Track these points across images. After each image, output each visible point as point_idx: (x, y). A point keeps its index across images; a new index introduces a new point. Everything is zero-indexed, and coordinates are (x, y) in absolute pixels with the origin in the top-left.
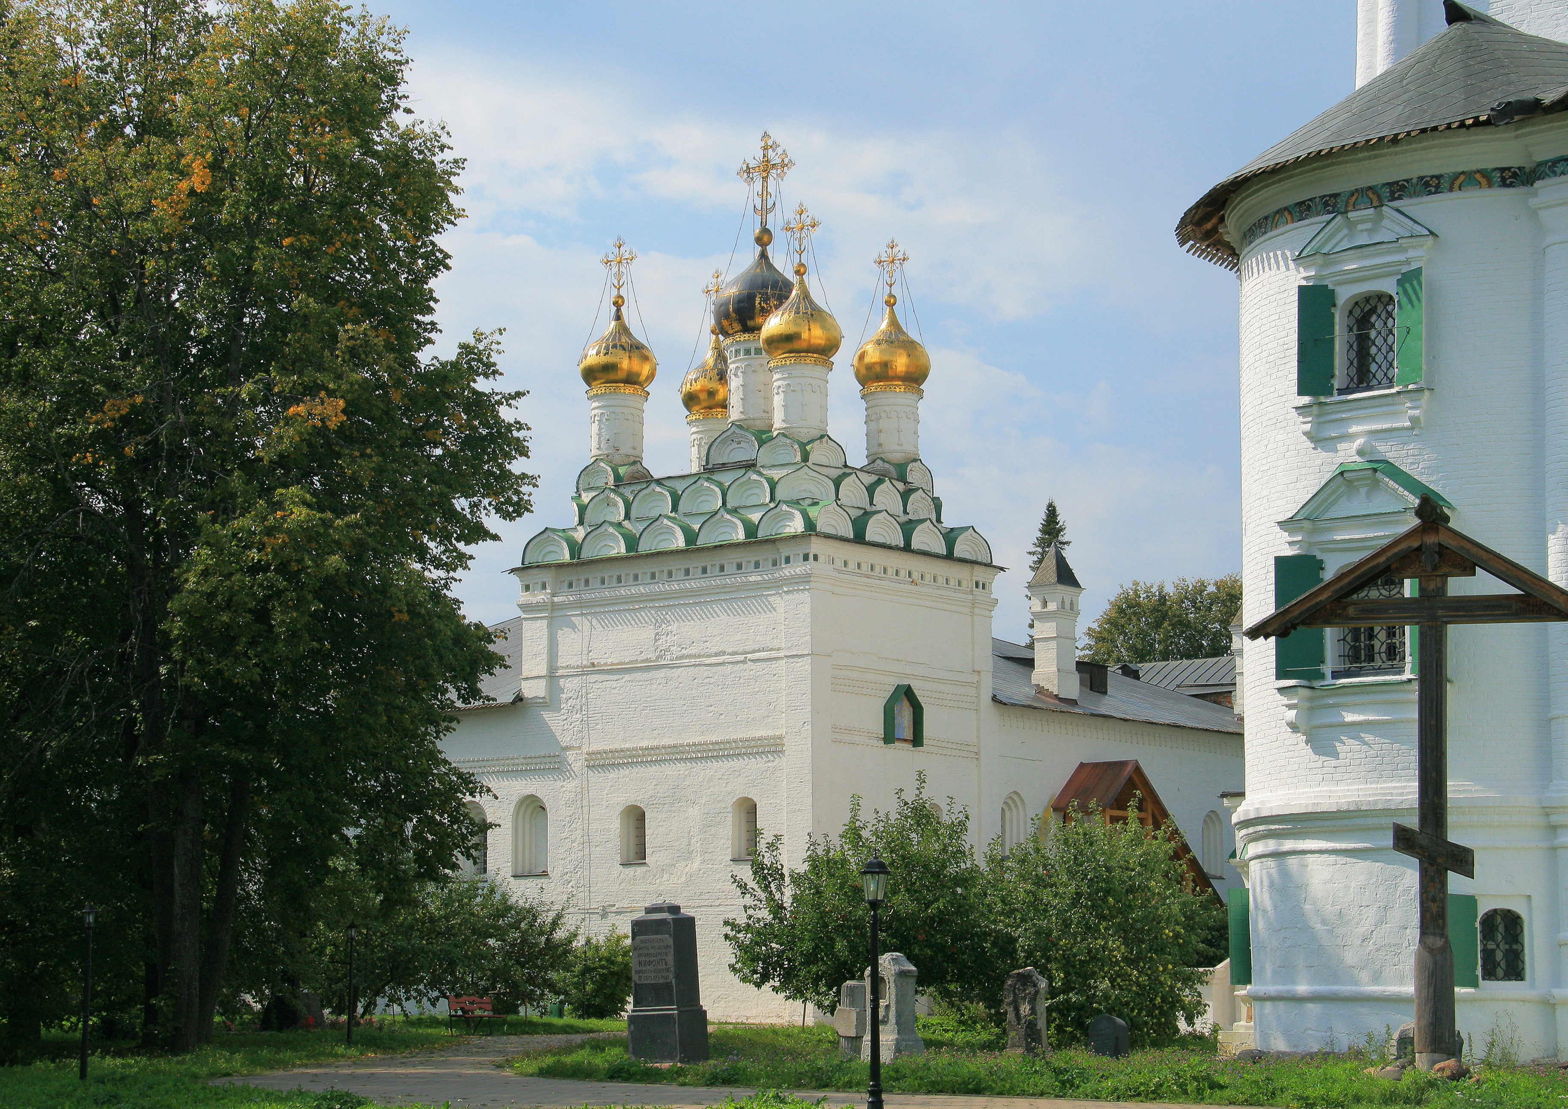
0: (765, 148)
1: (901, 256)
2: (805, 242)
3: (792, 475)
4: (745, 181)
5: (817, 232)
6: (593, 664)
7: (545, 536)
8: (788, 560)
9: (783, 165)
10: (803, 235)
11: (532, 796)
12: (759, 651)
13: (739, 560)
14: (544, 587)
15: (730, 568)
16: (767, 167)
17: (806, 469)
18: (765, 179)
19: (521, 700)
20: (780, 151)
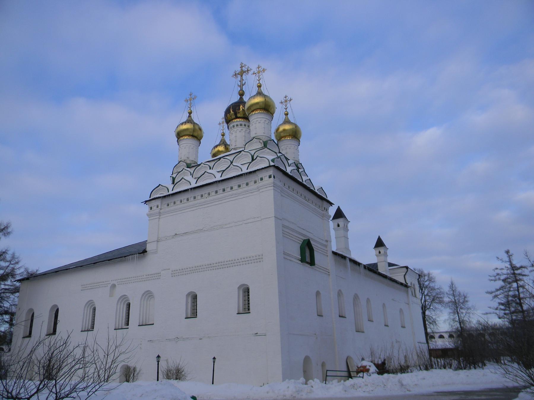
0: (242, 67)
1: (289, 99)
2: (261, 77)
3: (261, 151)
4: (235, 78)
5: (264, 74)
6: (176, 234)
7: (159, 188)
8: (262, 179)
9: (248, 70)
10: (260, 74)
11: (149, 291)
12: (249, 219)
13: (239, 184)
14: (158, 207)
15: (235, 187)
16: (242, 73)
17: (266, 149)
18: (242, 76)
19: (146, 252)
20: (247, 67)
